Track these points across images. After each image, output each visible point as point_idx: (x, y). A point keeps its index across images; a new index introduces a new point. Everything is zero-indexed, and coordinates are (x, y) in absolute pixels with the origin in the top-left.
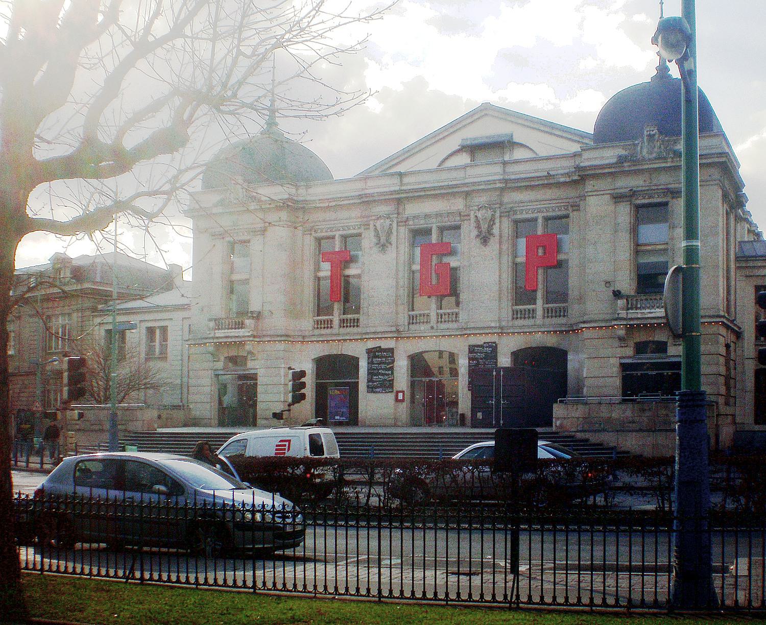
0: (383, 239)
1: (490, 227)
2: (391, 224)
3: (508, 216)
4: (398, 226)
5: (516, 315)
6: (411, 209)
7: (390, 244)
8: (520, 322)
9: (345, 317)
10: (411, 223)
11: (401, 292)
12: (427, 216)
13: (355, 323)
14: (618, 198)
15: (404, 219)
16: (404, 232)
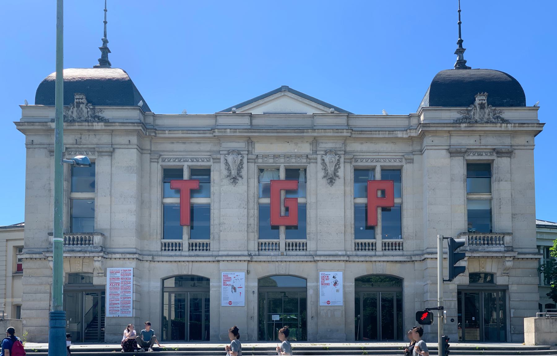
0: (234, 173)
1: (336, 170)
2: (241, 160)
3: (351, 163)
4: (248, 162)
5: (359, 247)
6: (260, 148)
7: (241, 177)
8: (360, 253)
9: (194, 241)
10: (260, 160)
11: (252, 221)
12: (275, 156)
13: (206, 247)
14: (453, 152)
15: (254, 157)
16: (253, 168)
